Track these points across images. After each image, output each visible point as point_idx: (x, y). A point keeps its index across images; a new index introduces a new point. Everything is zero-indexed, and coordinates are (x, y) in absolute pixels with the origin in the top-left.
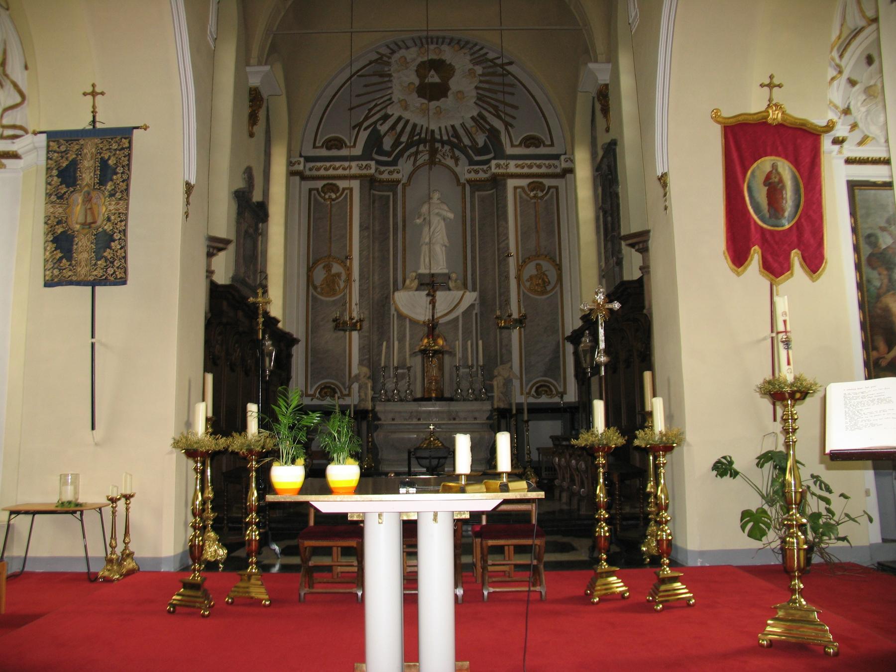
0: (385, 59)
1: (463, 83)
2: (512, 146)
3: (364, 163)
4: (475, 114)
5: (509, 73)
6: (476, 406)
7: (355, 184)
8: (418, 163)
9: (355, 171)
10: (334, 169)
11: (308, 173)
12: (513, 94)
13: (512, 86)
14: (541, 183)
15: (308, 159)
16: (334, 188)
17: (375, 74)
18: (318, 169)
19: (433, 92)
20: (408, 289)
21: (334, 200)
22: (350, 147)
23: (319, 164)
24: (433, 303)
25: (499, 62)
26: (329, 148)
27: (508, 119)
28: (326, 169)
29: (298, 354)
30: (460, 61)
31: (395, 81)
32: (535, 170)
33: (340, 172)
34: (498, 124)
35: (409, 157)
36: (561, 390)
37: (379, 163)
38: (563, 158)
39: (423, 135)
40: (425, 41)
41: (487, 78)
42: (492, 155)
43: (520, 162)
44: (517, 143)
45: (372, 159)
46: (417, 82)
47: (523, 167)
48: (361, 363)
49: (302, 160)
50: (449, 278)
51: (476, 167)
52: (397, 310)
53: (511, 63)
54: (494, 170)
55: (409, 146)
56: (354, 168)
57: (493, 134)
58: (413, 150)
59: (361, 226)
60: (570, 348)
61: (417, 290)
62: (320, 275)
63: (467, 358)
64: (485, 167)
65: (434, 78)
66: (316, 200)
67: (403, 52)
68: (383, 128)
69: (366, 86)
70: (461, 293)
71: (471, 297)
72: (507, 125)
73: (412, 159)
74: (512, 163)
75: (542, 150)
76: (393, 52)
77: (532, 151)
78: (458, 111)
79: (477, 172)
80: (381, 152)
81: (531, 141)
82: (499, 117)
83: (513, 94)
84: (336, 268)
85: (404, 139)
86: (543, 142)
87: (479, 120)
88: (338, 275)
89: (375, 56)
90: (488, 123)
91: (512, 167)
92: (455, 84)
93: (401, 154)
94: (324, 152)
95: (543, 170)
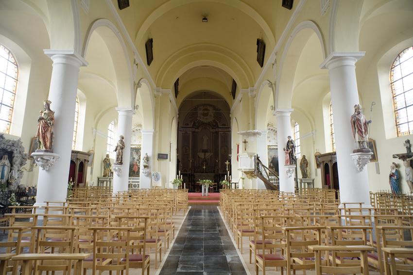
6: (212, 174)
7: (191, 132)
16: (187, 133)
19: (205, 115)
24: (205, 155)
30: (211, 109)
34: (218, 122)
40: (204, 105)
56: (191, 129)
57: (216, 123)
65: (206, 112)
68: (196, 122)
72: (220, 122)
77: (224, 127)
87: (214, 121)
91: (220, 130)
94: (185, 126)
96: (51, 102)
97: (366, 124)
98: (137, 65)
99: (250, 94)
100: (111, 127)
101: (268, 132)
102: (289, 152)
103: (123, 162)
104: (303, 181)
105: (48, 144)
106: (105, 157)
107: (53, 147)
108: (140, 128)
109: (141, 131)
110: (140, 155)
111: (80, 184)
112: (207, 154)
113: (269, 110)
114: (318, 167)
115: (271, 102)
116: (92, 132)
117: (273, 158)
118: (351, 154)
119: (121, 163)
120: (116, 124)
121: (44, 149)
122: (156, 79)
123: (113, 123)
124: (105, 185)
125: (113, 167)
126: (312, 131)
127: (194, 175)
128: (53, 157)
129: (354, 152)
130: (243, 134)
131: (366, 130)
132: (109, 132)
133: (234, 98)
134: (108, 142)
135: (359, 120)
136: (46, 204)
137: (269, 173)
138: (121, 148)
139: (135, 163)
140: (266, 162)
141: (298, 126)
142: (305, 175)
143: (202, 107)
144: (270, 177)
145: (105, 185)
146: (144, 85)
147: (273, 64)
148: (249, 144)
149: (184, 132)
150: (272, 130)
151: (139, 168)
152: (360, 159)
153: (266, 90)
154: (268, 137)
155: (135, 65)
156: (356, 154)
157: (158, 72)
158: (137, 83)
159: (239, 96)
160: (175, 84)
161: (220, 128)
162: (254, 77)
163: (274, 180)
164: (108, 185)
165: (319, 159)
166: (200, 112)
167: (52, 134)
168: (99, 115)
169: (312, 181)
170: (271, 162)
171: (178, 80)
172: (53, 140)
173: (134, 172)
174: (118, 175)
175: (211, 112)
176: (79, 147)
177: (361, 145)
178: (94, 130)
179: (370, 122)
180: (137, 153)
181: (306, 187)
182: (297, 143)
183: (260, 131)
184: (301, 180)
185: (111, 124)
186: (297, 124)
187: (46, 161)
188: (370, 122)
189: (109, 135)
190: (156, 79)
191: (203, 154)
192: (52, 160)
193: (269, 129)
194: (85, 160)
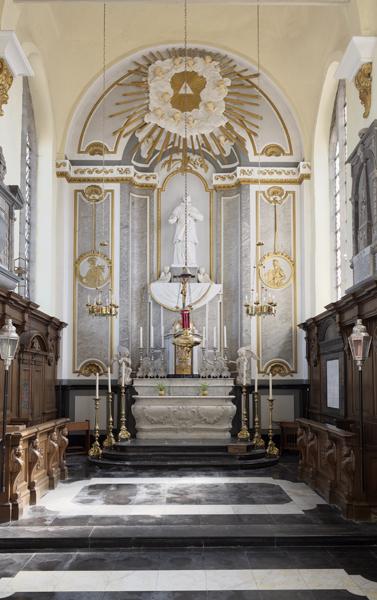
0: (144, 70)
1: (215, 95)
2: (256, 154)
3: (124, 167)
4: (223, 124)
5: (253, 85)
6: (219, 383)
8: (171, 171)
9: (116, 174)
10: (97, 172)
11: (72, 175)
12: (257, 105)
13: (257, 97)
14: (281, 188)
15: (73, 163)
16: (96, 190)
17: (134, 83)
18: (82, 172)
19: (185, 103)
21: (98, 201)
22: (112, 153)
23: (83, 167)
24: (183, 293)
25: (245, 74)
26: (92, 154)
27: (255, 130)
28: (90, 172)
29: (66, 335)
31: (151, 91)
32: (275, 177)
34: (243, 134)
35: (164, 165)
36: (292, 369)
37: (136, 168)
38: (301, 164)
39: (176, 144)
41: (236, 90)
42: (236, 164)
43: (263, 169)
44: (261, 151)
45: (132, 164)
46: (171, 92)
47: (265, 174)
48: (121, 343)
49: (68, 162)
50: (199, 272)
51: (222, 174)
52: (153, 299)
53: (257, 75)
54: (240, 176)
55: (164, 155)
56: (115, 172)
58: (167, 158)
59: (121, 224)
60: (303, 334)
61: (170, 281)
63: (213, 341)
64: (231, 174)
66: (80, 199)
67: (159, 62)
68: (141, 136)
69: (125, 95)
70: (208, 284)
71: (217, 289)
72: (250, 133)
73: (166, 166)
74: (256, 169)
75: (282, 159)
77: (273, 159)
78: (207, 123)
79: (224, 178)
80: (139, 159)
81: (276, 150)
82: (245, 127)
83: (257, 105)
84: (100, 261)
85: (158, 147)
86: (283, 151)
88: (102, 268)
90: (235, 133)
91: (256, 173)
95: (283, 177)
112: (195, 290)
127: (130, 389)
149: (84, 186)
161: (255, 165)
166: (160, 87)
175: (215, 95)
191: (177, 286)
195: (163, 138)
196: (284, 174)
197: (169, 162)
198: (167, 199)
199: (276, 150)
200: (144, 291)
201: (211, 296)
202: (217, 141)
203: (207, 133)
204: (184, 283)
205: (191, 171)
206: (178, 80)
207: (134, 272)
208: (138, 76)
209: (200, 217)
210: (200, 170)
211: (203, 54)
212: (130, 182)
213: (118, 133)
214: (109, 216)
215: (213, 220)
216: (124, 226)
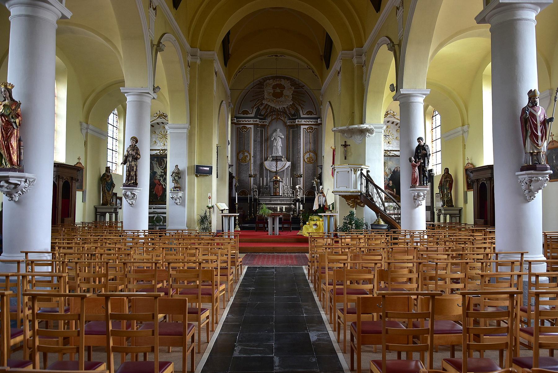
7: (252, 126)
9: (252, 122)
16: (245, 127)
19: (277, 95)
20: (269, 160)
32: (310, 123)
33: (247, 122)
48: (254, 184)
62: (241, 156)
65: (278, 90)
71: (288, 164)
72: (302, 108)
76: (264, 81)
80: (261, 115)
84: (246, 154)
85: (268, 110)
88: (247, 156)
89: (259, 82)
91: (303, 122)
92: (286, 92)
93: (267, 115)
94: (242, 115)
95: (313, 123)
96: (13, 87)
97: (546, 122)
98: (155, 9)
99: (355, 61)
100: (112, 118)
101: (385, 127)
102: (418, 165)
103: (138, 182)
104: (443, 212)
105: (15, 158)
106: (103, 171)
107: (23, 163)
108: (163, 120)
109: (166, 127)
110: (166, 167)
111: (66, 219)
113: (388, 94)
114: (468, 189)
115: (391, 78)
116: (81, 129)
117: (394, 171)
118: (517, 173)
119: (135, 184)
120: (122, 114)
121: (9, 166)
122: (189, 30)
123: (116, 112)
124: (107, 219)
125: (119, 190)
126: (463, 125)
128: (24, 180)
129: (522, 170)
130: (343, 132)
131: (544, 134)
132: (110, 127)
133: (328, 67)
134: (110, 146)
135: (533, 116)
136: (24, 254)
137: (385, 198)
138: (132, 157)
139: (157, 181)
140: (380, 180)
141: (438, 117)
142: (448, 203)
143: (273, 82)
144: (386, 204)
145: (107, 219)
146: (169, 43)
147: (398, 9)
148: (352, 149)
150: (393, 123)
151: (164, 190)
152: (531, 181)
153: (384, 59)
154: (385, 136)
155: (152, 9)
156: (524, 172)
157: (193, 20)
158: (156, 43)
159: (336, 65)
160: (223, 42)
162: (365, 34)
163: (394, 208)
164: (114, 220)
165: (472, 175)
166: (268, 91)
167: (19, 141)
168: (94, 105)
169: (458, 212)
170: (390, 179)
171: (229, 33)
172: (22, 151)
173: (157, 196)
174: (131, 205)
175: (288, 92)
176: (61, 157)
177: (535, 158)
178: (85, 125)
179: (551, 119)
180: (160, 165)
181: (448, 221)
182: (434, 147)
183: (372, 127)
184: (440, 210)
185: (112, 114)
186: (437, 113)
187: (13, 186)
188: (551, 119)
189: (110, 134)
190: (189, 30)
191: (274, 163)
192: (23, 184)
193: (388, 122)
194: (72, 179)
195: (270, 108)
196: (311, 122)
197: (272, 115)
198: (270, 131)
199: (310, 113)
200: (262, 165)
201: (286, 167)
202: (289, 110)
203: (285, 106)
204: (277, 162)
205: (279, 119)
206: (274, 87)
207: (258, 157)
208: (261, 85)
209: (283, 137)
210: (283, 118)
211: (284, 78)
212: (257, 124)
213: (253, 108)
214: (249, 137)
215: (287, 138)
216: (255, 141)
